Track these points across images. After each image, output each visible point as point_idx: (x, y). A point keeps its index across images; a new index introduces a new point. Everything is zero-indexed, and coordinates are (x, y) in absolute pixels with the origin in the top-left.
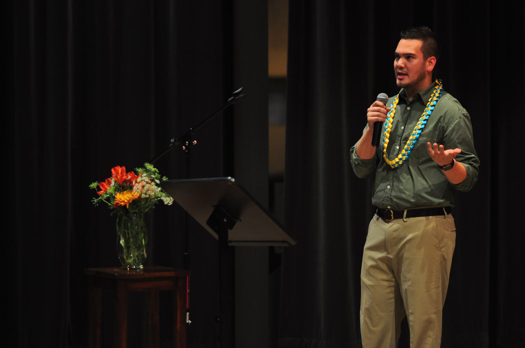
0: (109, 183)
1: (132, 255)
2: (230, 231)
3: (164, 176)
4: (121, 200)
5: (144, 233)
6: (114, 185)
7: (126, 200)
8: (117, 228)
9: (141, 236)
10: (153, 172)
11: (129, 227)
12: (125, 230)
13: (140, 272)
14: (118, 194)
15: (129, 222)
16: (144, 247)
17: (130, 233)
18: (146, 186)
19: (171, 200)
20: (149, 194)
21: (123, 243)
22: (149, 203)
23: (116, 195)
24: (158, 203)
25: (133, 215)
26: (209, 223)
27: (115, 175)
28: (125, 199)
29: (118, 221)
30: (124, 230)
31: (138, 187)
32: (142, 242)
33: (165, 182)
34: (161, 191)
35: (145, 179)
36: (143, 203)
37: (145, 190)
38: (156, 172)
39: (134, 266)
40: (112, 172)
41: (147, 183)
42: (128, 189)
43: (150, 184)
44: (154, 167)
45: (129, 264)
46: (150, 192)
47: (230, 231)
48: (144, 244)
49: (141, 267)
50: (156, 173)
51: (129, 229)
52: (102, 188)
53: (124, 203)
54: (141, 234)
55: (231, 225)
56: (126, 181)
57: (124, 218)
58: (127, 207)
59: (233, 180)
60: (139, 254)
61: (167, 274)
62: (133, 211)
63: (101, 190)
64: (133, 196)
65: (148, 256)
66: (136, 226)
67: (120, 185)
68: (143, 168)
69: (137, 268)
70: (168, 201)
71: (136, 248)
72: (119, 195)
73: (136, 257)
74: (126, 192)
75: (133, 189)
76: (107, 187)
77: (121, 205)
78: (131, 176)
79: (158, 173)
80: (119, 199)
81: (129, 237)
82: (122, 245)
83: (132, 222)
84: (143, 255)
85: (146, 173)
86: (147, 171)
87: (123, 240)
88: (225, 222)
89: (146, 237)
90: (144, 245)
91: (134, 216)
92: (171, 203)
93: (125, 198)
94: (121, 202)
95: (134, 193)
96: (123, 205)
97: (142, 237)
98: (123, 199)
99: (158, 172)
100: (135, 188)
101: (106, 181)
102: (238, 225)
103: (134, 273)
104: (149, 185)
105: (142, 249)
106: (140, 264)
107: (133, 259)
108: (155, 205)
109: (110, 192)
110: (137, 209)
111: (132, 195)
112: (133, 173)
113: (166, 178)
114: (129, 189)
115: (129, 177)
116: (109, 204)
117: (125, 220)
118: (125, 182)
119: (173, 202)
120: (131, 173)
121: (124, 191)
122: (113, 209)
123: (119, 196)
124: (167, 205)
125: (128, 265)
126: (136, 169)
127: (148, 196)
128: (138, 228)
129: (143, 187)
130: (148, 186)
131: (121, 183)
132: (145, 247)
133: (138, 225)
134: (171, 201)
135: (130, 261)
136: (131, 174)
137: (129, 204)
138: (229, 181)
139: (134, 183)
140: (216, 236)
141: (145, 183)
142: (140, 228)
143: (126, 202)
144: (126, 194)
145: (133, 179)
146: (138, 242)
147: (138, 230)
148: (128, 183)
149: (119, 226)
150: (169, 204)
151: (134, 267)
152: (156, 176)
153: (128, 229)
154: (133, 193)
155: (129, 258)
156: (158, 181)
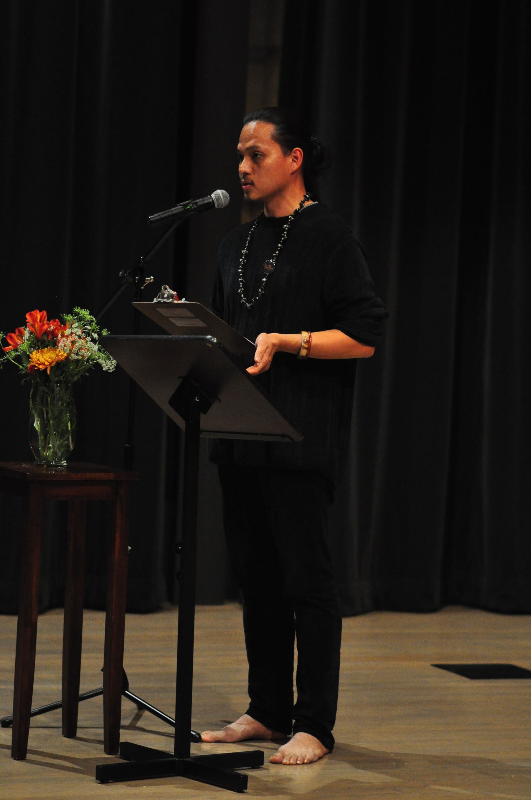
0: (21, 335)
1: (50, 445)
4: (40, 362)
5: (70, 413)
6: (28, 338)
7: (47, 361)
8: (31, 403)
9: (66, 417)
11: (49, 402)
12: (43, 406)
13: (62, 471)
14: (34, 353)
16: (69, 434)
17: (50, 412)
18: (78, 342)
19: (112, 365)
20: (81, 354)
21: (38, 426)
22: (80, 367)
23: (32, 353)
24: (93, 368)
25: (55, 385)
26: (172, 402)
27: (30, 324)
28: (45, 360)
30: (42, 407)
31: (66, 343)
32: (67, 427)
33: (105, 338)
34: (99, 350)
36: (71, 367)
37: (76, 348)
38: (93, 321)
39: (54, 462)
40: (26, 319)
41: (80, 337)
42: (50, 346)
43: (84, 339)
44: (90, 314)
45: (46, 458)
46: (83, 351)
47: (202, 416)
48: (70, 429)
49: (64, 463)
50: (93, 324)
51: (49, 405)
52: (10, 342)
54: (66, 414)
55: (205, 407)
56: (46, 333)
57: (42, 388)
58: (48, 372)
60: (62, 443)
61: (103, 476)
63: (9, 345)
64: (57, 356)
66: (59, 401)
67: (38, 339)
68: (74, 315)
69: (58, 465)
70: (109, 366)
72: (37, 353)
73: (57, 448)
74: (48, 350)
75: (58, 346)
76: (17, 340)
77: (40, 369)
78: (55, 326)
79: (96, 323)
80: (36, 359)
81: (47, 417)
82: (37, 429)
83: (53, 395)
84: (69, 446)
85: (78, 322)
86: (80, 319)
87: (39, 422)
89: (74, 419)
90: (70, 430)
91: (57, 386)
92: (113, 368)
93: (45, 358)
94: (40, 365)
95: (59, 352)
96: (42, 368)
98: (42, 360)
100: (61, 344)
101: (17, 331)
102: (215, 408)
103: (53, 472)
105: (66, 437)
106: (63, 459)
107: (52, 450)
108: (89, 370)
110: (62, 376)
111: (56, 354)
112: (58, 321)
113: (108, 332)
116: (21, 367)
117: (43, 391)
118: (46, 335)
119: (117, 367)
121: (44, 349)
122: (26, 375)
123: (36, 356)
124: (106, 371)
125: (45, 459)
126: (63, 316)
127: (80, 357)
128: (62, 404)
129: (73, 343)
130: (80, 342)
132: (71, 434)
133: (61, 401)
134: (113, 366)
136: (54, 323)
137: (51, 367)
138: (209, 341)
139: (60, 336)
140: (181, 423)
141: (77, 337)
142: (65, 405)
143: (46, 365)
144: (47, 353)
145: (58, 330)
147: (62, 408)
148: (50, 336)
149: (34, 400)
150: (109, 370)
151: (53, 463)
152: (93, 327)
154: (57, 352)
156: (96, 336)
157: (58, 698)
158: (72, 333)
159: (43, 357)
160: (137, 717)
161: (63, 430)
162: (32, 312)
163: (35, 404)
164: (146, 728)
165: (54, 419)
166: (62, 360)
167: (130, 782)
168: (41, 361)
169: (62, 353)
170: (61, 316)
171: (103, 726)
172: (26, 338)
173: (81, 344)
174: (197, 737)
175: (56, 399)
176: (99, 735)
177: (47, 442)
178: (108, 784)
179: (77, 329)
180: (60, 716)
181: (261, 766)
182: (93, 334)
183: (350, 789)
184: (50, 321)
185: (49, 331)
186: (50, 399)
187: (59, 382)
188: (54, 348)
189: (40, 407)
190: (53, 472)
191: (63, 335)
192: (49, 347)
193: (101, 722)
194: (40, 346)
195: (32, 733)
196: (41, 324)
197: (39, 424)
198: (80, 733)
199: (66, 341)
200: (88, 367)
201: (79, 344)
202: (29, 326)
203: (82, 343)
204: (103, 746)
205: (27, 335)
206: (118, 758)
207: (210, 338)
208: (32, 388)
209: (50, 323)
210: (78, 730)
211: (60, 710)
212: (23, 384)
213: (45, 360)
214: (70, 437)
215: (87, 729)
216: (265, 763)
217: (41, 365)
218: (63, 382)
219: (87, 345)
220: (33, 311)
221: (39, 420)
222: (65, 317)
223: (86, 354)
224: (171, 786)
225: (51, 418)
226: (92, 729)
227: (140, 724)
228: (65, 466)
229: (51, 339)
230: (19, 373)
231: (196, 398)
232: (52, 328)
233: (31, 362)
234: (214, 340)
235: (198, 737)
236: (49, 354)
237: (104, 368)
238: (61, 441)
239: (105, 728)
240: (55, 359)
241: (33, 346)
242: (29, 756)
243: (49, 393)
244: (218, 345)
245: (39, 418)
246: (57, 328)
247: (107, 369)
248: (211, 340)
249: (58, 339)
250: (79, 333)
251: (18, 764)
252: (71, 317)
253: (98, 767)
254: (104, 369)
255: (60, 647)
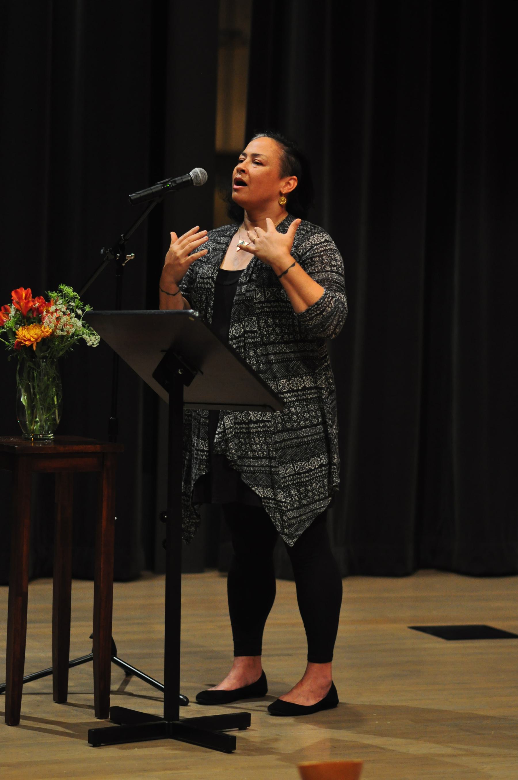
0: (7, 312)
1: (37, 419)
2: (185, 387)
3: (87, 305)
4: (26, 338)
5: (56, 387)
6: (13, 315)
7: (33, 338)
8: (18, 378)
9: (52, 392)
10: (72, 298)
12: (29, 381)
13: (49, 444)
14: (20, 329)
15: (35, 370)
17: (36, 387)
19: (96, 340)
20: (66, 330)
21: (25, 400)
24: (78, 344)
25: (41, 360)
26: (156, 375)
29: (19, 368)
31: (51, 320)
32: (53, 401)
34: (83, 326)
35: (62, 308)
36: (56, 343)
37: (61, 324)
38: (77, 298)
39: (41, 435)
40: (12, 296)
41: (64, 314)
42: (35, 322)
44: (74, 291)
45: (33, 431)
47: (185, 387)
48: (56, 403)
49: (51, 436)
53: (29, 343)
54: (52, 389)
55: (188, 379)
56: (32, 310)
57: (29, 364)
58: (34, 348)
59: (197, 314)
60: (49, 417)
61: (90, 448)
62: (42, 354)
64: (43, 332)
65: (60, 422)
66: (45, 376)
67: (23, 316)
68: (58, 292)
69: (45, 438)
71: (44, 409)
72: (23, 330)
73: (44, 422)
74: (33, 327)
75: (43, 323)
76: (3, 318)
77: (26, 345)
78: (40, 303)
79: (80, 300)
80: (22, 336)
82: (24, 403)
83: (39, 371)
84: (55, 420)
85: (62, 299)
87: (25, 397)
88: (179, 374)
89: (60, 393)
90: (56, 404)
91: (43, 362)
93: (31, 334)
94: (25, 341)
95: (45, 328)
96: (28, 345)
97: (54, 393)
98: (28, 336)
99: (79, 298)
100: (46, 320)
101: (2, 308)
102: (198, 380)
103: (41, 445)
104: (68, 317)
107: (39, 424)
108: (74, 345)
109: (8, 325)
111: (42, 330)
112: (42, 299)
113: (91, 308)
114: (36, 323)
115: (37, 305)
116: (7, 343)
117: (29, 367)
118: (32, 312)
119: (101, 342)
120: (40, 299)
121: (29, 325)
122: (12, 351)
123: (22, 332)
124: (91, 346)
125: (32, 433)
126: (48, 293)
127: (65, 333)
128: (48, 379)
129: (58, 319)
130: (65, 318)
131: (24, 312)
132: (57, 408)
134: (97, 341)
135: (36, 427)
136: (39, 300)
137: (37, 343)
138: (191, 315)
139: (45, 313)
140: (164, 395)
141: (61, 313)
142: (51, 379)
143: (32, 341)
144: (32, 329)
145: (43, 307)
146: (48, 400)
147: (49, 383)
148: (35, 313)
149: (21, 375)
150: (93, 345)
151: (40, 436)
153: (34, 380)
154: (43, 328)
155: (33, 423)
156: (80, 312)
157: (49, 665)
158: (56, 310)
159: (28, 334)
160: (126, 682)
161: (49, 404)
162: (18, 290)
163: (22, 380)
164: (135, 693)
165: (41, 393)
166: (48, 336)
167: (121, 745)
168: (27, 337)
169: (47, 329)
170: (45, 293)
171: (93, 691)
172: (12, 315)
173: (66, 320)
174: (184, 701)
175: (42, 374)
176: (89, 700)
177: (34, 416)
178: (101, 747)
179: (61, 306)
180: (51, 683)
181: (248, 728)
182: (77, 310)
183: (335, 747)
184: (34, 299)
185: (35, 308)
186: (37, 374)
187: (45, 357)
188: (39, 324)
189: (26, 382)
190: (41, 445)
191: (48, 312)
192: (34, 324)
193: (92, 689)
194: (26, 323)
195: (24, 699)
196: (26, 301)
197: (26, 399)
198: (70, 699)
199: (51, 318)
200: (73, 343)
201: (64, 320)
202: (15, 303)
203: (67, 319)
204: (93, 711)
205: (12, 312)
206: (108, 722)
207: (193, 312)
208: (19, 363)
209: (35, 301)
210: (69, 696)
211: (51, 677)
212: (9, 360)
213: (31, 336)
214: (286, 390)
215: (78, 695)
216: (251, 725)
217: (27, 342)
218: (48, 358)
219: (71, 322)
220: (19, 289)
221: (26, 394)
222: (50, 294)
223: (71, 330)
224: (162, 748)
225: (38, 392)
226: (82, 695)
227: (129, 688)
228: (52, 439)
229: (36, 316)
230: (6, 349)
231: (178, 371)
232: (37, 305)
233: (17, 338)
234: (196, 314)
235: (185, 700)
236: (35, 330)
237: (88, 343)
238: (48, 415)
239: (95, 693)
240: (41, 335)
241: (19, 323)
242: (22, 722)
243: (35, 368)
244: (200, 319)
245: (26, 393)
246: (41, 305)
247: (91, 344)
248: (193, 314)
249: (43, 316)
250: (64, 309)
251: (12, 730)
252: (56, 294)
253: (90, 731)
254: (88, 344)
255: (49, 616)
